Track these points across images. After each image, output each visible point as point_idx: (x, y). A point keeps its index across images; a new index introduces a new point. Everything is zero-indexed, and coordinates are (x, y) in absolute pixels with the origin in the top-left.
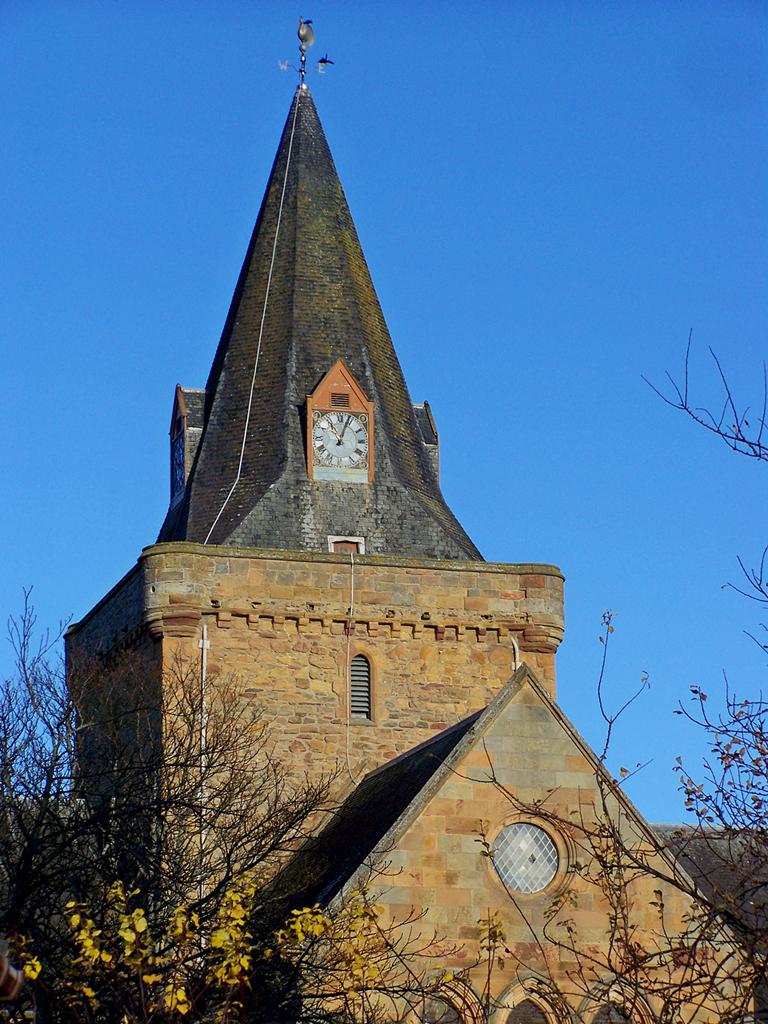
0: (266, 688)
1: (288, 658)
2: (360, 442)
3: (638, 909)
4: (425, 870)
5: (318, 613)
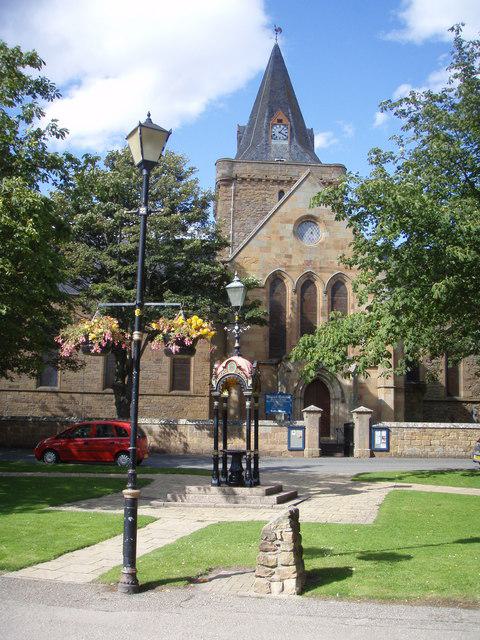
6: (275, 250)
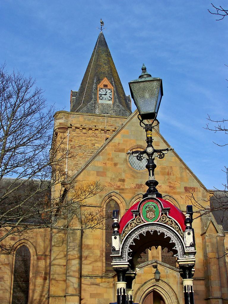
0: (84, 145)
1: (90, 138)
2: (110, 95)
3: (174, 175)
4: (108, 162)
5: (97, 128)
6: (110, 174)
